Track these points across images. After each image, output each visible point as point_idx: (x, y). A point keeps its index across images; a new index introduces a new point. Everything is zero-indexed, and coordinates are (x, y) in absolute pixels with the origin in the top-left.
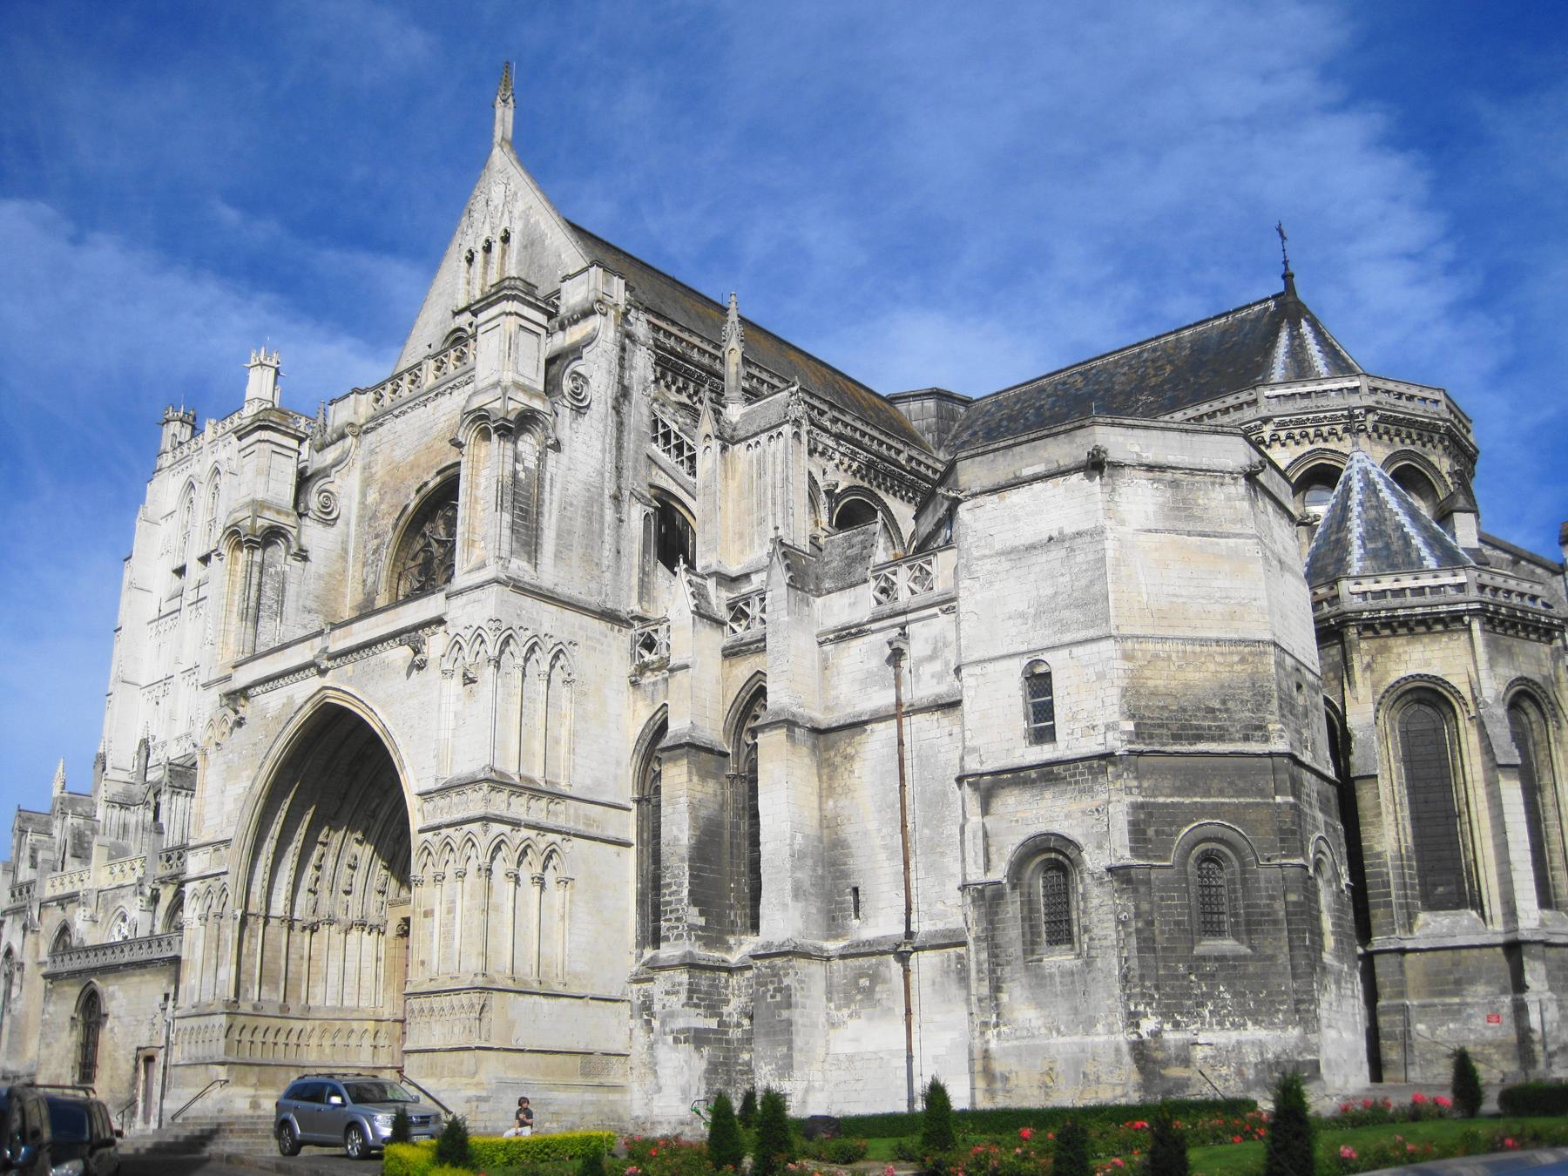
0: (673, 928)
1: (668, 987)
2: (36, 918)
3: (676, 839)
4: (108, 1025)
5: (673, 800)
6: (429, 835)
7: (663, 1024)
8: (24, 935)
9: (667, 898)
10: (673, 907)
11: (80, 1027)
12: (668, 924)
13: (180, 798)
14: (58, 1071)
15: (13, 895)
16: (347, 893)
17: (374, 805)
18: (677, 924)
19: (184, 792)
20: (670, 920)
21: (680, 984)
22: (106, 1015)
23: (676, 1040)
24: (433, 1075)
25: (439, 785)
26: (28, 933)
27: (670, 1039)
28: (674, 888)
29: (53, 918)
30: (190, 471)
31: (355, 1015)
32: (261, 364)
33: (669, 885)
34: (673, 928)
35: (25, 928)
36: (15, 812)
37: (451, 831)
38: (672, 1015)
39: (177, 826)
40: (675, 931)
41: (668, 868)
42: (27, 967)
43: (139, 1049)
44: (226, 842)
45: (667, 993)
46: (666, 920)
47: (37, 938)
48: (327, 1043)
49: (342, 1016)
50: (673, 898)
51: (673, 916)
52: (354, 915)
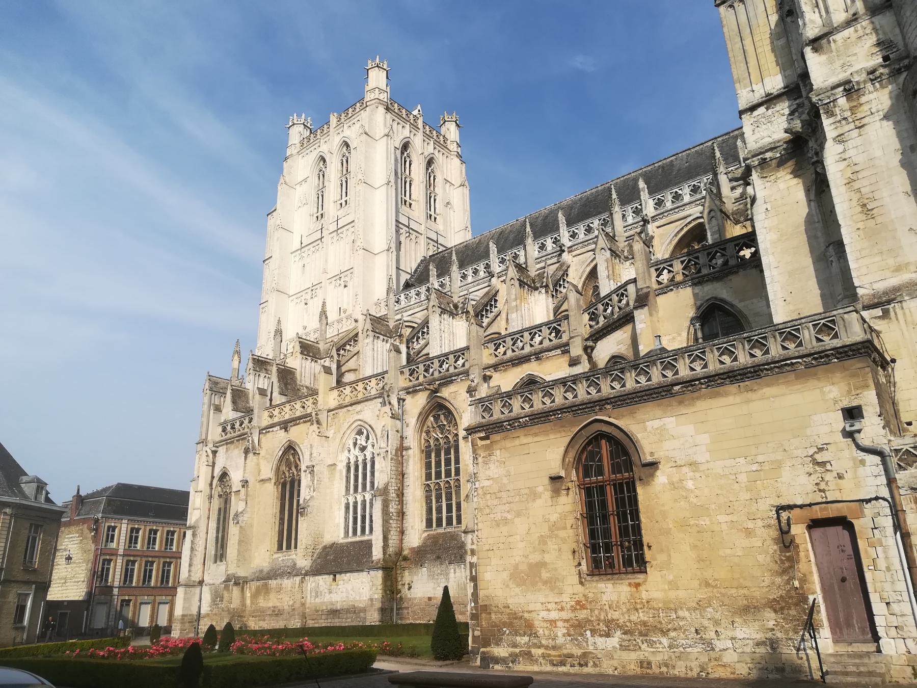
2: (256, 442)
4: (661, 478)
8: (246, 458)
11: (574, 490)
13: (380, 342)
14: (535, 558)
15: (224, 430)
19: (382, 337)
22: (653, 465)
26: (251, 455)
29: (276, 440)
30: (320, 149)
32: (377, 66)
35: (247, 451)
36: (206, 377)
39: (379, 363)
42: (250, 484)
43: (780, 509)
47: (258, 459)
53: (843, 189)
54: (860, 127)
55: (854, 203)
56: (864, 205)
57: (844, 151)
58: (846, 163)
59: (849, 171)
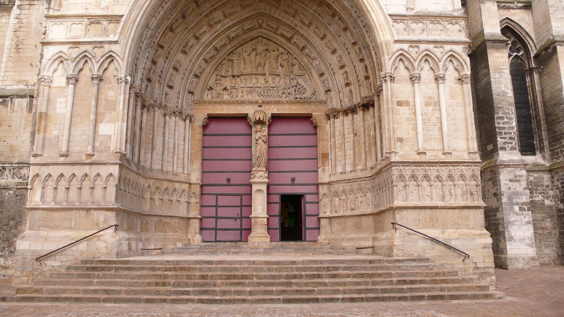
0: (508, 143)
1: (511, 177)
3: (504, 93)
5: (499, 70)
6: (405, 46)
7: (510, 198)
9: (501, 125)
10: (507, 131)
12: (504, 140)
16: (171, 87)
17: (203, 30)
18: (510, 141)
20: (505, 138)
21: (521, 176)
23: (521, 209)
24: (433, 227)
25: (412, 13)
27: (517, 208)
28: (506, 120)
31: (177, 178)
33: (502, 118)
34: (508, 143)
37: (431, 47)
38: (517, 194)
40: (510, 145)
41: (500, 108)
44: (115, 19)
45: (511, 181)
46: (502, 138)
48: (157, 197)
49: (170, 177)
50: (505, 126)
51: (508, 136)
52: (172, 105)
53: (12, 33)
54: (30, 5)
55: (14, 43)
56: (17, 45)
57: (20, 14)
58: (18, 20)
59: (18, 25)
